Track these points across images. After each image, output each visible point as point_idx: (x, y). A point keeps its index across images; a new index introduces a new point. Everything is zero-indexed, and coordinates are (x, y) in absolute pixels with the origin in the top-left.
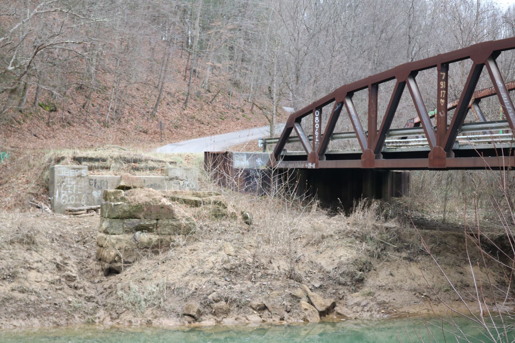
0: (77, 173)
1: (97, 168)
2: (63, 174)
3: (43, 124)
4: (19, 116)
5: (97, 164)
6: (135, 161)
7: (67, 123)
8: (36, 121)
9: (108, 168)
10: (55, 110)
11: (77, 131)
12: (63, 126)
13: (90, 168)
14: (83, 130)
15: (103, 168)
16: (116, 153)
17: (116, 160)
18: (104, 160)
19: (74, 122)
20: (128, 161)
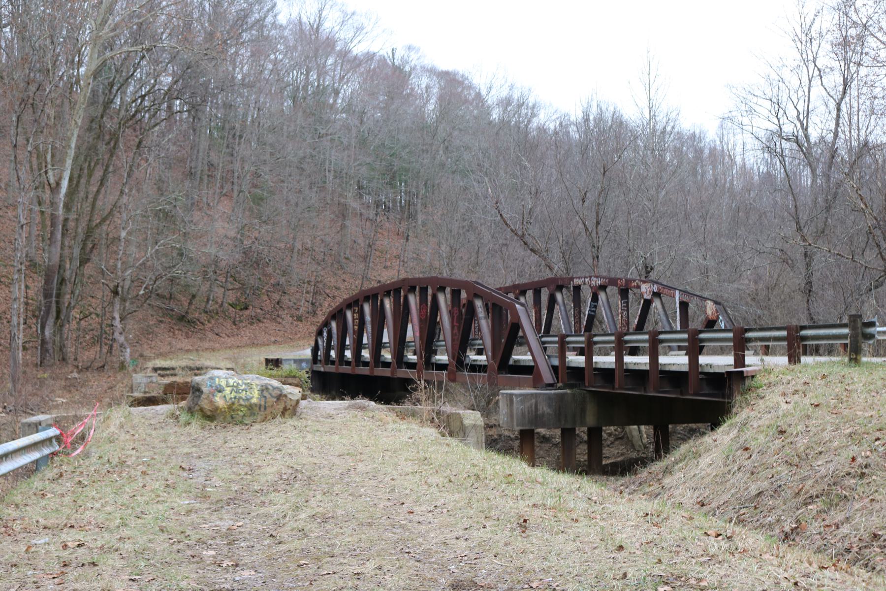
0: (149, 380)
1: (167, 375)
2: (139, 381)
3: (228, 324)
4: (204, 317)
5: (168, 372)
6: (198, 369)
7: (256, 320)
8: (221, 320)
9: (175, 375)
10: (246, 308)
11: (266, 327)
12: (252, 324)
13: (163, 376)
14: (272, 326)
15: (172, 375)
16: (184, 363)
17: (183, 369)
18: (173, 369)
19: (264, 318)
20: (191, 369)
